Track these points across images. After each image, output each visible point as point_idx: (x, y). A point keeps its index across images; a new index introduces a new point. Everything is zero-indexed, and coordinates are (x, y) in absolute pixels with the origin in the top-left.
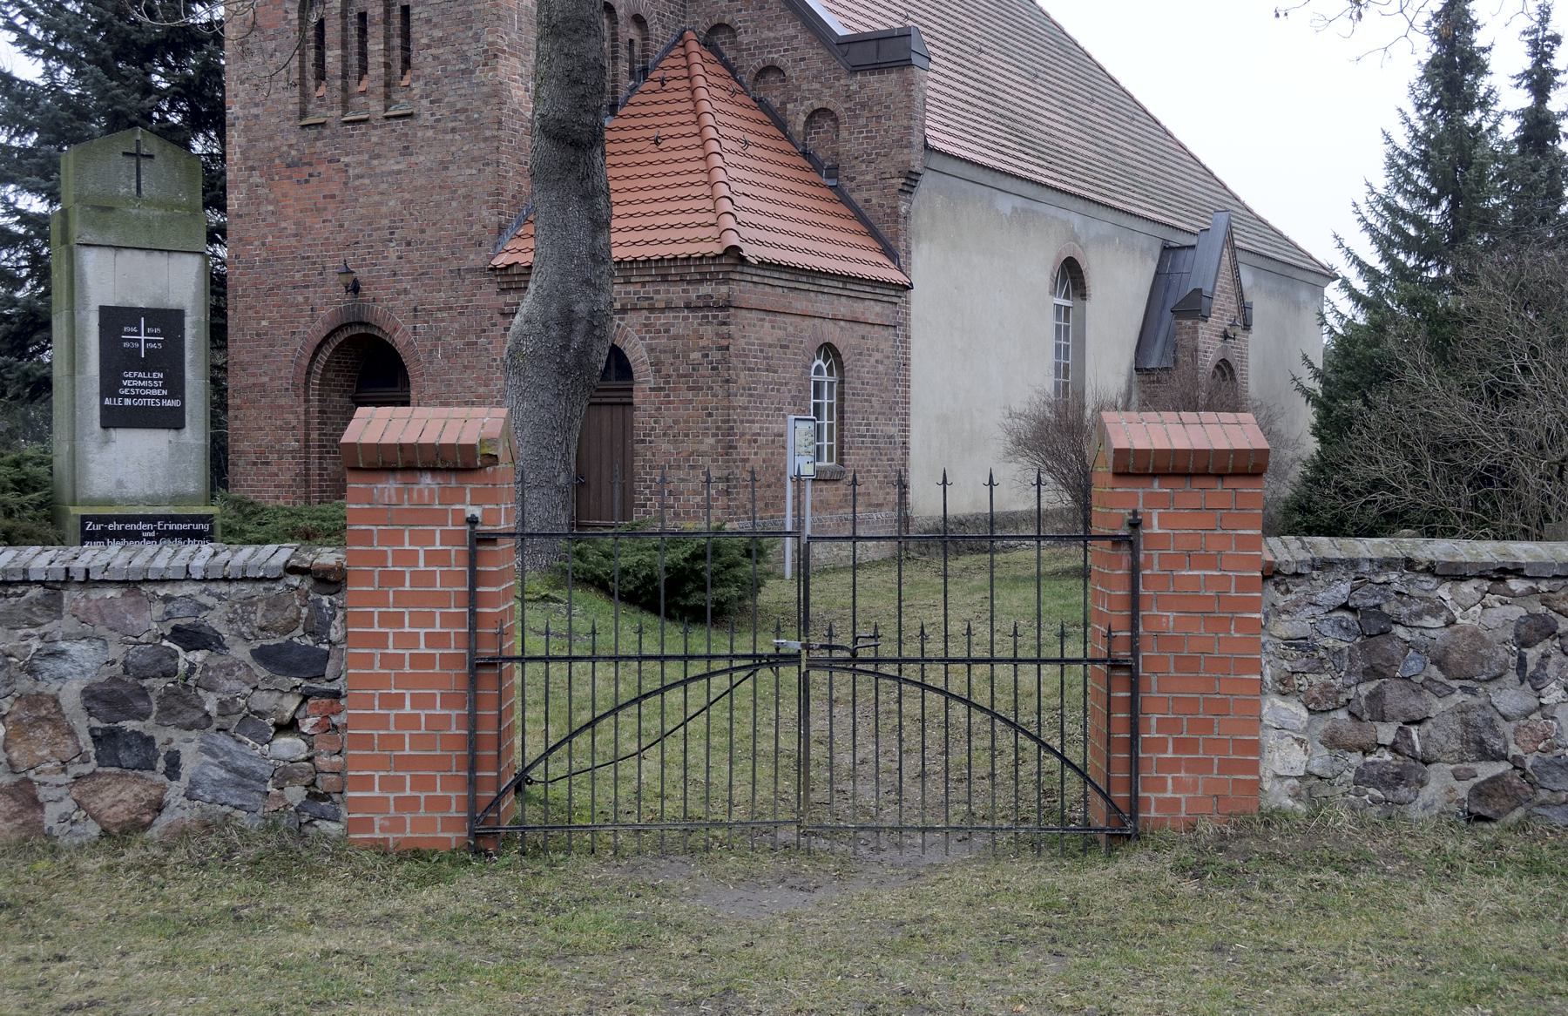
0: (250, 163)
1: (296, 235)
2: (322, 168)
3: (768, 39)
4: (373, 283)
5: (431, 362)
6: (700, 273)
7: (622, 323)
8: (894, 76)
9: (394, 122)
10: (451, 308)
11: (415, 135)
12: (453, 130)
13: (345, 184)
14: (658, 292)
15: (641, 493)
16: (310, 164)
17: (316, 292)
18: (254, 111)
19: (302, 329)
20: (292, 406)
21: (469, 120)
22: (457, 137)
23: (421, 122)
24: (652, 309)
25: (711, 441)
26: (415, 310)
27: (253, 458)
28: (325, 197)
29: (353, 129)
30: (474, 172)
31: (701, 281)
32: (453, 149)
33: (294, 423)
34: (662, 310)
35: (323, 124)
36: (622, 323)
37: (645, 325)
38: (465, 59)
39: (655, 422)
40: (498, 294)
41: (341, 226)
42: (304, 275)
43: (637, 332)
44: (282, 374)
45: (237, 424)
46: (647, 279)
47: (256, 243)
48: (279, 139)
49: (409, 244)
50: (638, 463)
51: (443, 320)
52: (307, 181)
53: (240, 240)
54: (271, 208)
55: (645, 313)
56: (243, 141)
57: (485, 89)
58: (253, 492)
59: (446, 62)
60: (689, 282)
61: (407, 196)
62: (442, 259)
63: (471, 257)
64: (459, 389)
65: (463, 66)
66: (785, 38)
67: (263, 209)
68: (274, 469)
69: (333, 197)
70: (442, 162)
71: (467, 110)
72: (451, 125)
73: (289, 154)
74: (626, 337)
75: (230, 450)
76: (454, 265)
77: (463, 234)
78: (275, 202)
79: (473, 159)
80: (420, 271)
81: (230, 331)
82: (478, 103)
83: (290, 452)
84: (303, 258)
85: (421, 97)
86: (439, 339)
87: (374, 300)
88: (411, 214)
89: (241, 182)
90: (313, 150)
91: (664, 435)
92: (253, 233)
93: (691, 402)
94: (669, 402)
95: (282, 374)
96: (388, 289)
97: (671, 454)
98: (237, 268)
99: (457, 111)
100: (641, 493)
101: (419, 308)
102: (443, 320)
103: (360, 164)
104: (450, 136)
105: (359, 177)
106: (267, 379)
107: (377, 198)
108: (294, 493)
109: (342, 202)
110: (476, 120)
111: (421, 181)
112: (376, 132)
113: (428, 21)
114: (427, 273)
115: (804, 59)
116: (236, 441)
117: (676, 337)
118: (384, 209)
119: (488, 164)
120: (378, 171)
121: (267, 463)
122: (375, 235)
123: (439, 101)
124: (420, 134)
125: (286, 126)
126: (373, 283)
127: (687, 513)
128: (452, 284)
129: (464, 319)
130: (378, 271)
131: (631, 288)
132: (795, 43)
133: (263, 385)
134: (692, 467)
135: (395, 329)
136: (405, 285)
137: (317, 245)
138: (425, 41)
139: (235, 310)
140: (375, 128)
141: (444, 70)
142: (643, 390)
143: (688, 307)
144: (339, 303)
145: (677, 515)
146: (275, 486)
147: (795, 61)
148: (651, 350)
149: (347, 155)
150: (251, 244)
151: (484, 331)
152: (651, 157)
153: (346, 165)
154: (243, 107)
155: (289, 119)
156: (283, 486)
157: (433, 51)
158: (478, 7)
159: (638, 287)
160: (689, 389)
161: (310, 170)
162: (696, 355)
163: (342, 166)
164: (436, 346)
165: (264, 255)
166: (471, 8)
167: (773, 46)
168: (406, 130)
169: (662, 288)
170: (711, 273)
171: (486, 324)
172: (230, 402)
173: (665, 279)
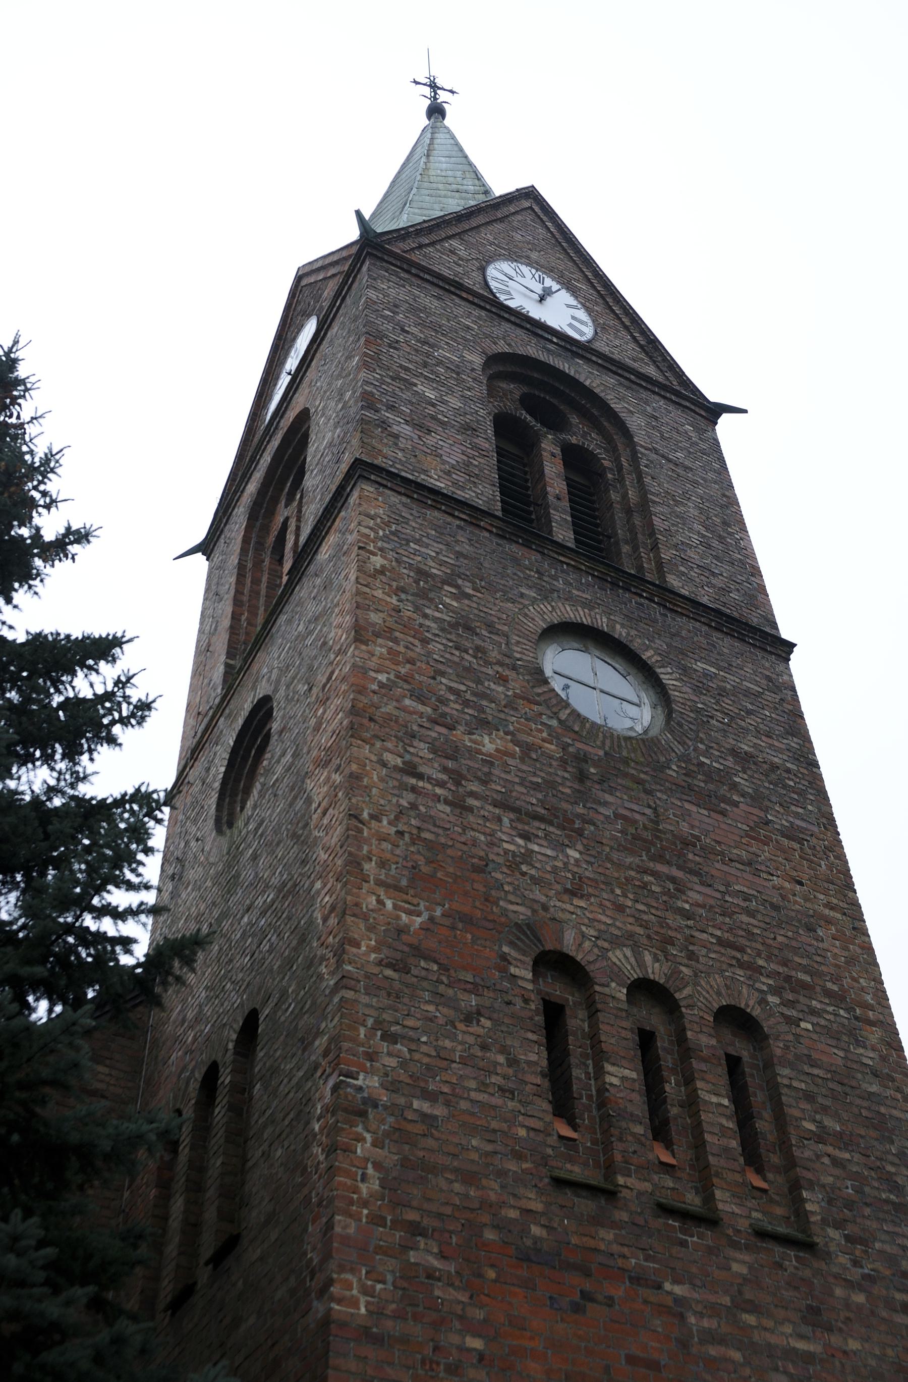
0: (412, 1216)
2: (619, 1291)
9: (778, 1249)
28: (631, 1360)
52: (577, 1308)
54: (476, 1343)
56: (389, 1156)
89: (379, 1250)
105: (711, 1337)
125: (512, 1166)
141: (859, 1191)
154: (393, 1086)
155: (519, 1156)
161: (587, 1287)
163: (669, 1301)
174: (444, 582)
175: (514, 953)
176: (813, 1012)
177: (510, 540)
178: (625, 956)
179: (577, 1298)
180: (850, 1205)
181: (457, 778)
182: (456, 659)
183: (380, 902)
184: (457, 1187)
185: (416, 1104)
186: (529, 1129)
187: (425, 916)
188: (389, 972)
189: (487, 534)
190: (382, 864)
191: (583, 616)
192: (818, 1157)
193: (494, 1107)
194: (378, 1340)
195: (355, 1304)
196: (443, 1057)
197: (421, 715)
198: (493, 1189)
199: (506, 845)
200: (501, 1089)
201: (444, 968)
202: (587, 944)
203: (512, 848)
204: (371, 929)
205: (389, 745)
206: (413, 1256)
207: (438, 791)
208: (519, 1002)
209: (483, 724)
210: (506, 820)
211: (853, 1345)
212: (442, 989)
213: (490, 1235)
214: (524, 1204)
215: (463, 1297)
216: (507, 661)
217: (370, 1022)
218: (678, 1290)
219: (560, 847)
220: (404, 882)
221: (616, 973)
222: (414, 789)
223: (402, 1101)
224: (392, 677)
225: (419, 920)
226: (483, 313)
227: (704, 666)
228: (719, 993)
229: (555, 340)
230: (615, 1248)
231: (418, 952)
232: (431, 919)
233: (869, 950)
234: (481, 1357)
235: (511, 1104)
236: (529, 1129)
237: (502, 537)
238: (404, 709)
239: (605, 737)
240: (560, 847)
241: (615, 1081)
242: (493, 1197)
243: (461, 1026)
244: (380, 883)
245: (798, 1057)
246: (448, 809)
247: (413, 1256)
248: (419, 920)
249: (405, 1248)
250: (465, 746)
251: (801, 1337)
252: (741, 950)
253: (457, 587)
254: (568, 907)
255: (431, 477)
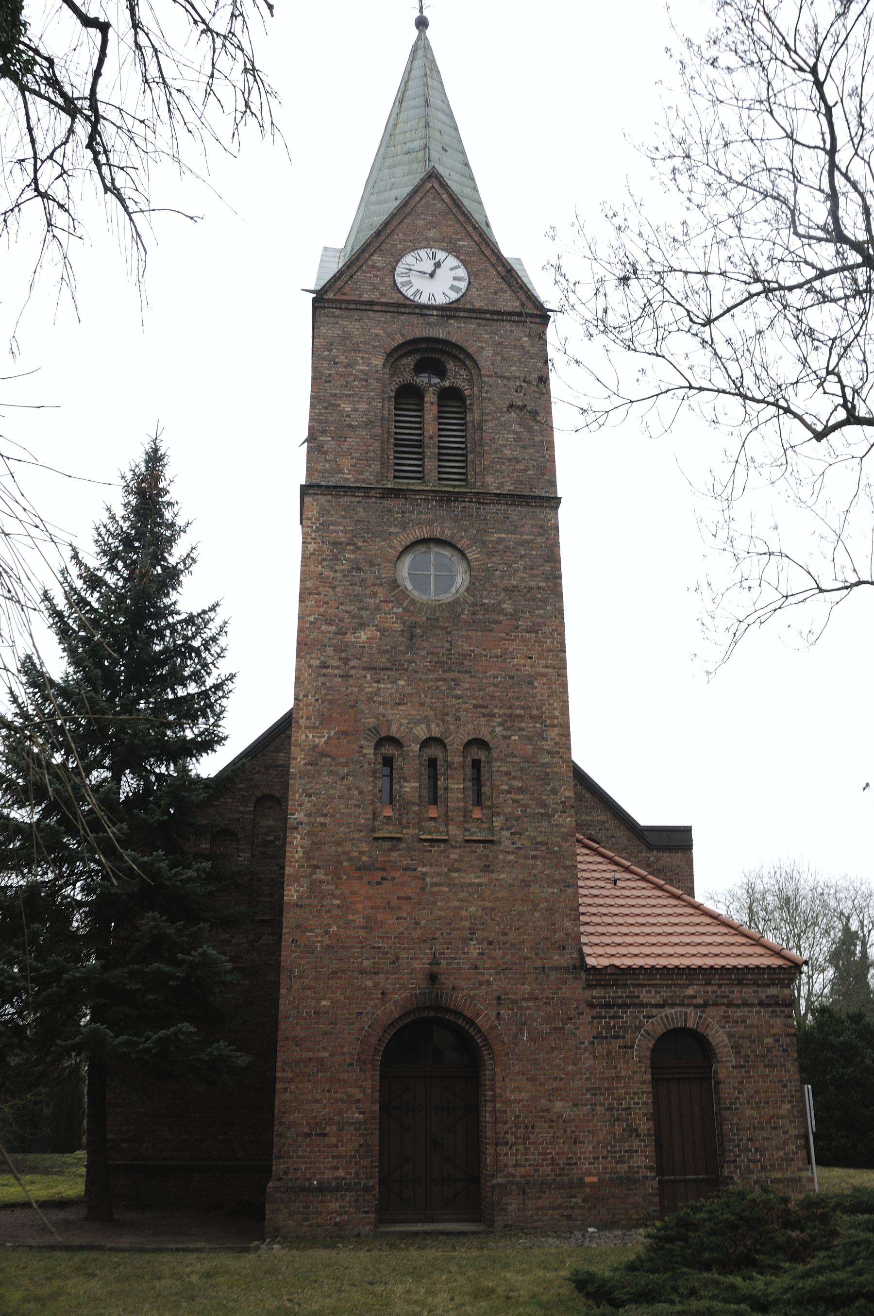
0: (315, 862)
1: (366, 928)
2: (397, 874)
3: (586, 820)
4: (453, 974)
5: (516, 1044)
6: (770, 979)
7: (704, 1015)
8: (680, 855)
9: (475, 845)
10: (536, 999)
11: (497, 858)
12: (534, 857)
13: (423, 889)
14: (733, 992)
15: (730, 1151)
16: (384, 870)
17: (388, 978)
18: (322, 820)
19: (369, 1009)
20: (356, 1081)
21: (549, 851)
22: (538, 863)
23: (501, 848)
24: (730, 1005)
25: (789, 1106)
26: (499, 998)
27: (307, 1130)
28: (399, 898)
29: (430, 846)
30: (556, 891)
31: (768, 986)
32: (535, 871)
33: (361, 1096)
34: (738, 1006)
35: (399, 839)
36: (704, 1015)
37: (724, 1017)
38: (544, 805)
39: (739, 1093)
40: (584, 989)
41: (418, 924)
42: (374, 963)
43: (718, 1022)
44: (345, 1050)
45: (287, 1096)
46: (726, 982)
47: (318, 931)
48: (348, 846)
49: (490, 943)
50: (727, 1126)
51: (528, 1008)
52: (379, 883)
53: (299, 927)
54: (337, 902)
55: (723, 1008)
56: (307, 842)
57: (564, 830)
58: (303, 1163)
59: (526, 806)
60: (758, 986)
61: (488, 904)
62: (525, 958)
63: (555, 958)
64: (546, 1067)
65: (542, 811)
66: (598, 821)
67: (327, 902)
68: (333, 1140)
69: (409, 898)
70: (523, 881)
71: (547, 844)
72: (532, 853)
73: (360, 859)
74: (708, 1026)
75: (276, 1122)
76: (539, 963)
77: (547, 939)
78: (342, 897)
79: (555, 881)
80: (504, 966)
81: (281, 1008)
82: (559, 839)
83: (352, 1124)
84: (373, 948)
85: (502, 829)
86: (525, 1024)
87: (454, 988)
88: (492, 919)
89: (301, 877)
90: (387, 859)
91: (748, 1102)
92: (313, 922)
93: (768, 1076)
94: (750, 1077)
95: (345, 1050)
96: (469, 979)
97: (754, 1118)
98: (295, 952)
99: (537, 843)
100: (730, 1151)
101: (503, 997)
102: (528, 1008)
103: (439, 874)
104: (531, 862)
106: (327, 1054)
107: (457, 904)
108: (357, 1163)
109: (419, 904)
110: (556, 851)
111: (504, 894)
112: (455, 851)
113: (508, 774)
114: (511, 969)
115: (614, 837)
116: (284, 1113)
117: (751, 1026)
118: (464, 913)
119: (569, 886)
120: (456, 881)
121: (324, 1135)
122: (455, 934)
123: (520, 834)
124: (501, 857)
125: (357, 836)
126: (453, 974)
127: (772, 1165)
128: (537, 979)
129: (550, 1008)
130: (459, 964)
131: (709, 989)
132: (607, 825)
133: (321, 1060)
134: (775, 1128)
135: (478, 1015)
136: (486, 977)
137: (389, 938)
138: (505, 787)
139: (289, 990)
140: (454, 847)
142: (726, 1068)
143: (761, 1004)
144: (415, 989)
145: (764, 1168)
146: (333, 1157)
147: (607, 837)
148: (730, 1036)
149: (424, 865)
150: (312, 931)
151: (571, 1019)
152: (606, 893)
153: (424, 874)
154: (308, 815)
155: (360, 831)
156: (343, 1157)
157: (513, 796)
158: (555, 770)
159: (715, 988)
160: (765, 1066)
161: (384, 875)
162: (769, 1041)
163: (419, 874)
164: (521, 1031)
165: (327, 942)
166: (548, 770)
167: (590, 825)
168: (487, 852)
169: (736, 989)
170: (779, 979)
171: (572, 1013)
172: (278, 1074)
173: (740, 983)
174: (347, 544)
175: (366, 743)
176: (521, 729)
177: (387, 498)
178: (422, 729)
179: (379, 879)
180: (517, 819)
181: (346, 661)
182: (350, 592)
183: (307, 736)
184: (333, 848)
185: (318, 820)
186: (366, 819)
187: (326, 737)
188: (309, 767)
189: (374, 500)
190: (308, 718)
191: (424, 533)
192: (505, 801)
193: (350, 814)
194: (301, 906)
195: (293, 896)
196: (331, 798)
197: (330, 633)
198: (348, 846)
199: (367, 690)
200: (355, 806)
201: (334, 759)
202: (403, 728)
203: (370, 690)
204: (302, 750)
205: (313, 655)
206: (314, 877)
207: (336, 672)
208: (366, 765)
209: (362, 626)
210: (369, 676)
211: (503, 876)
212: (332, 768)
213: (345, 864)
214: (361, 849)
215: (333, 887)
216: (378, 582)
217: (301, 790)
218: (424, 870)
219: (394, 682)
220: (317, 724)
221: (415, 739)
222: (324, 675)
223: (313, 820)
224: (316, 616)
225: (323, 740)
226: (388, 316)
227: (499, 535)
228: (468, 734)
229: (435, 313)
230: (398, 858)
231: (323, 755)
232: (329, 737)
233: (565, 686)
234: (339, 906)
235: (358, 811)
236: (366, 819)
237: (383, 498)
238: (322, 632)
239: (427, 609)
240: (394, 682)
241: (408, 789)
242: (348, 849)
243: (339, 783)
244: (306, 727)
245: (506, 755)
246: (340, 680)
247: (314, 877)
248: (323, 740)
249: (312, 874)
250: (351, 642)
251: (478, 877)
252: (486, 707)
253: (354, 544)
254: (396, 712)
255: (344, 473)
